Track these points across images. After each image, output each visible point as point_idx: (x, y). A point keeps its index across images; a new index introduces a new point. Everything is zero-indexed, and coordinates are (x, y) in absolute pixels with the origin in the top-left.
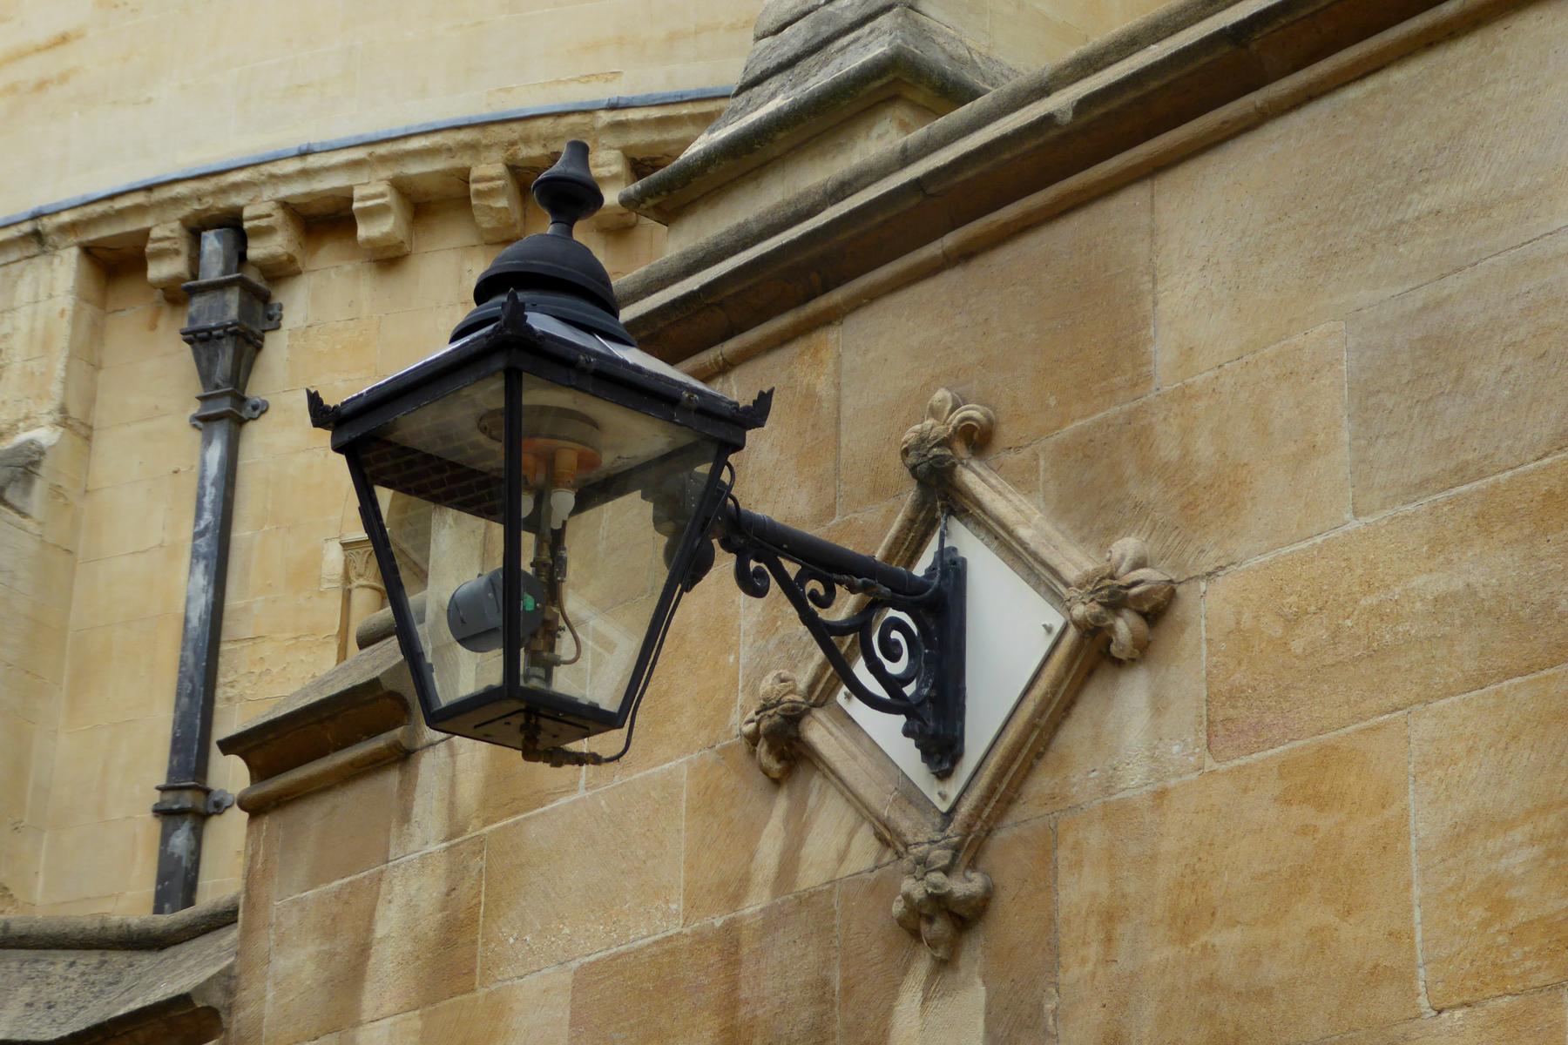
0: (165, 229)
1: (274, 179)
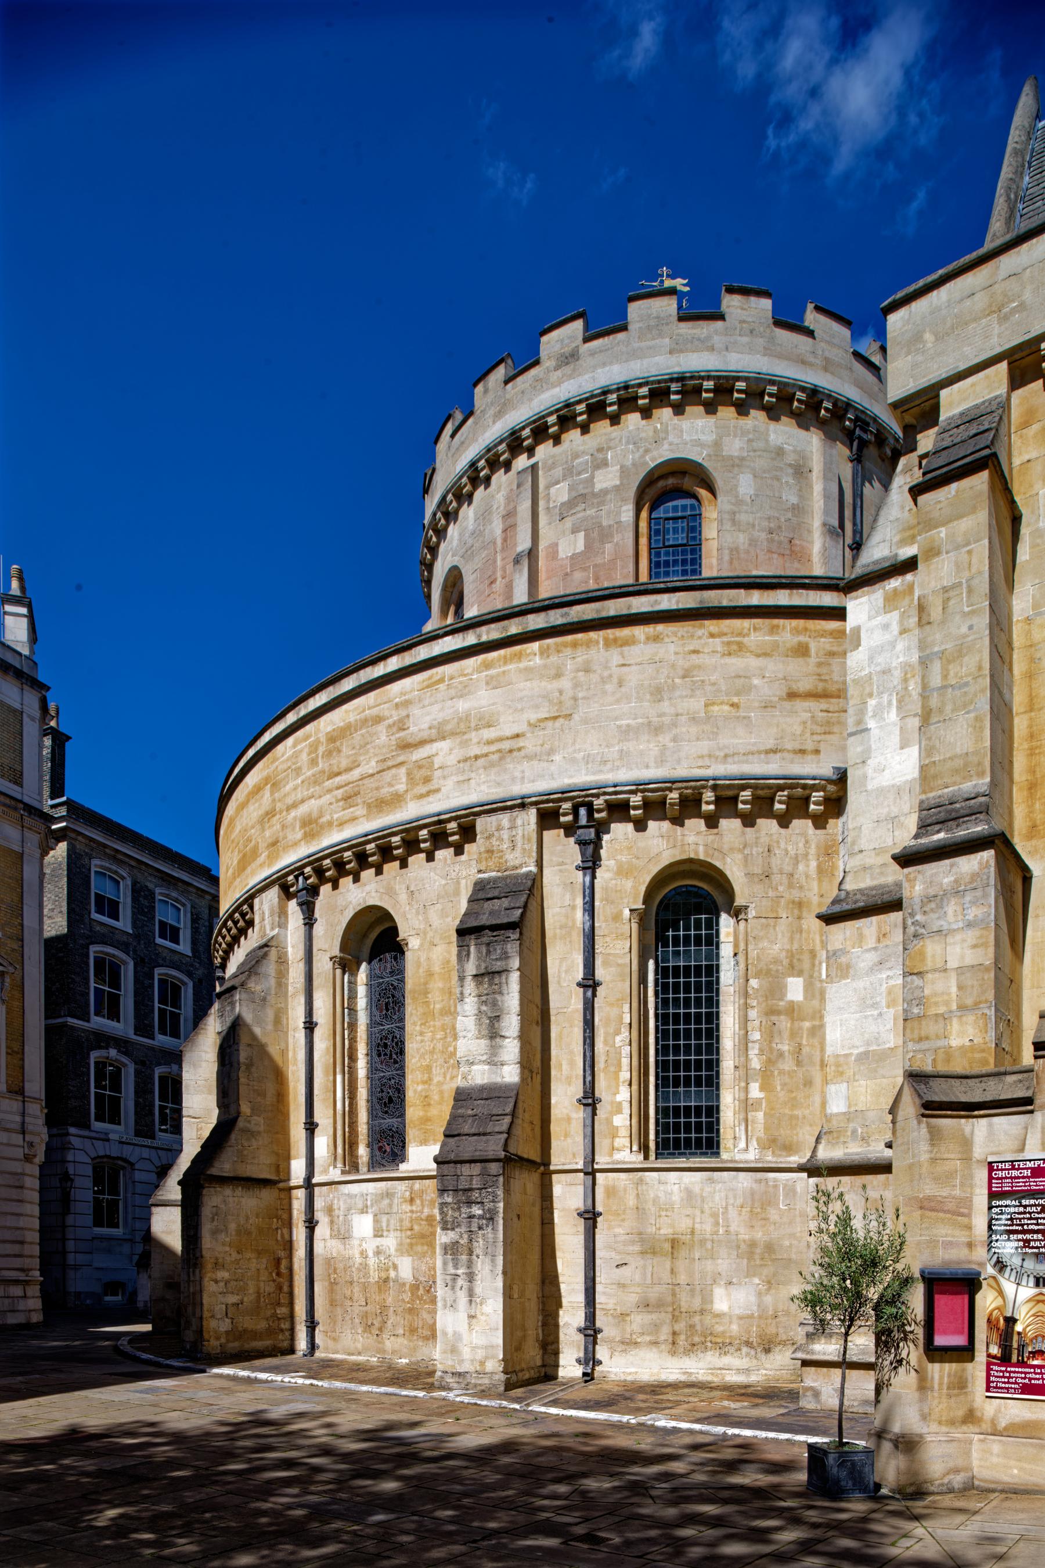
0: (567, 806)
1: (605, 794)
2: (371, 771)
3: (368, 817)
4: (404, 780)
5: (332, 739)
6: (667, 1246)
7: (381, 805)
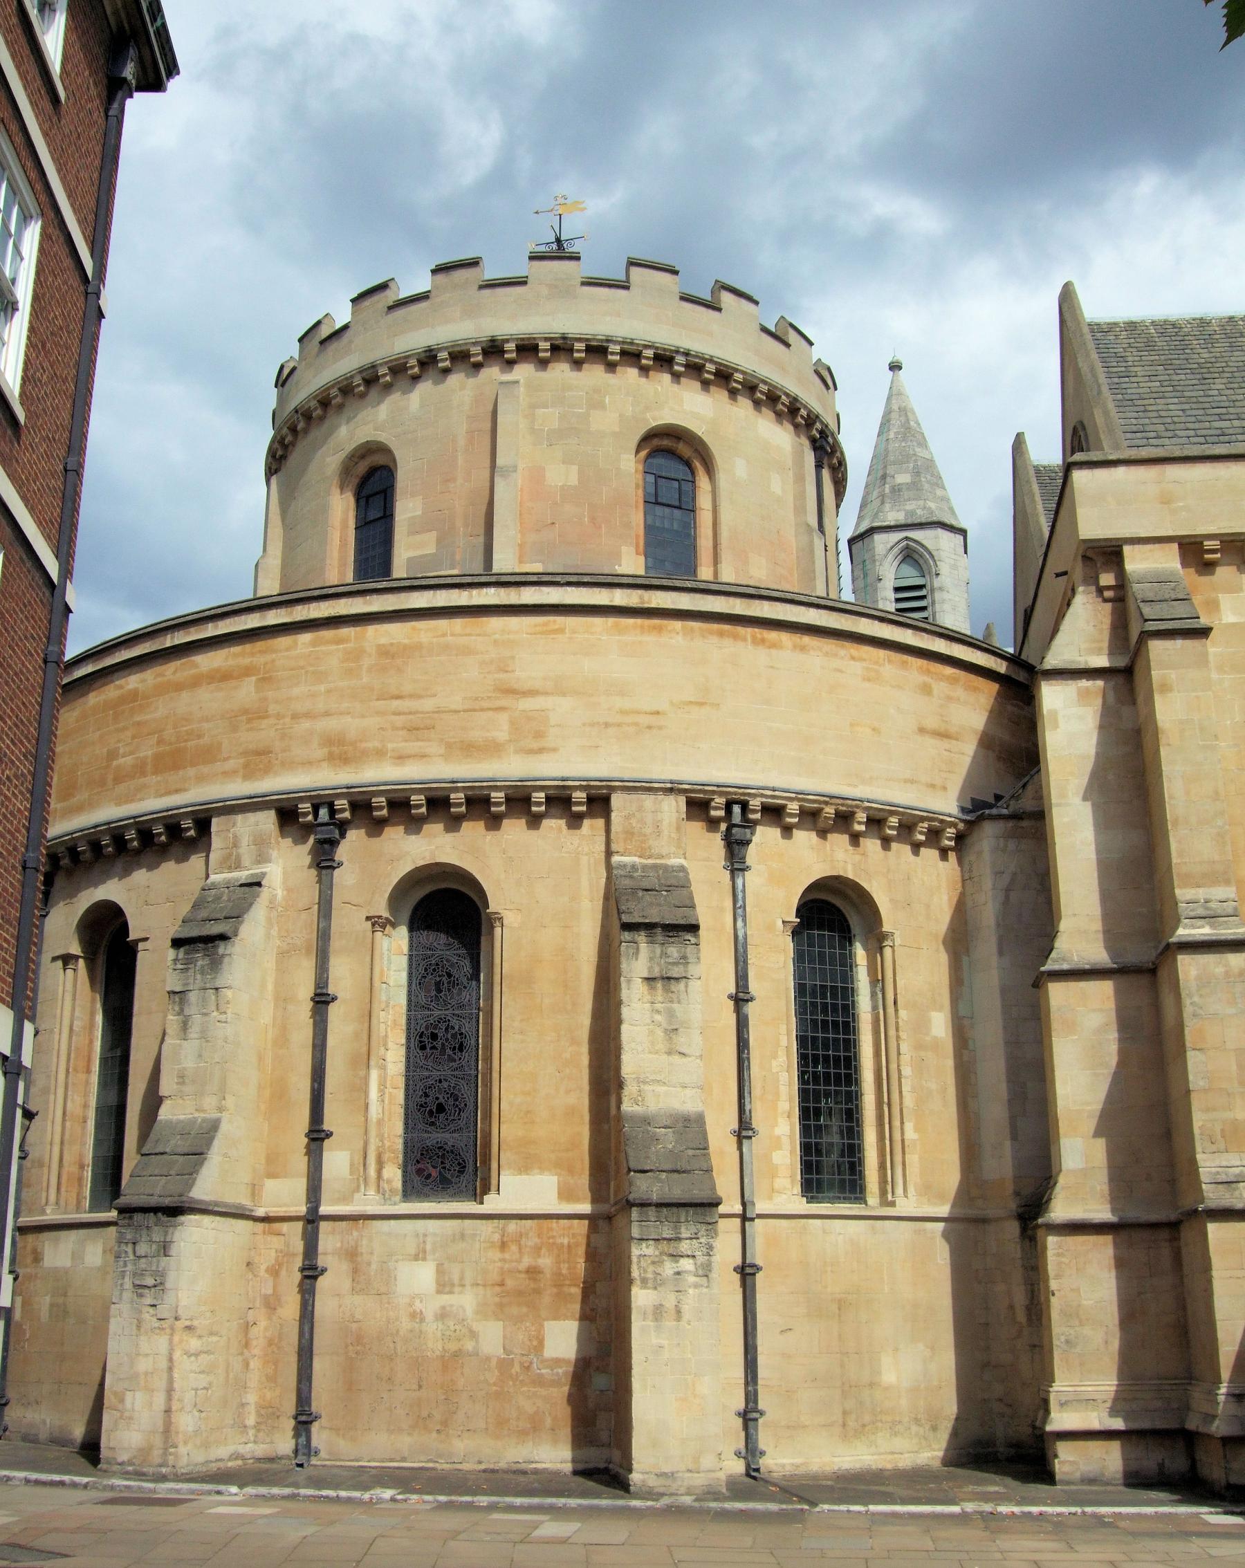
0: (720, 801)
1: (762, 796)
2: (454, 707)
3: (447, 757)
4: (506, 727)
5: (385, 652)
6: (834, 1307)
7: (469, 749)
